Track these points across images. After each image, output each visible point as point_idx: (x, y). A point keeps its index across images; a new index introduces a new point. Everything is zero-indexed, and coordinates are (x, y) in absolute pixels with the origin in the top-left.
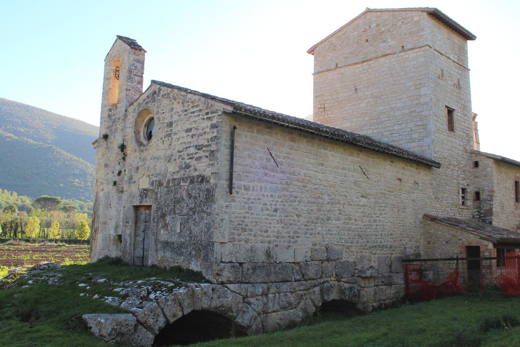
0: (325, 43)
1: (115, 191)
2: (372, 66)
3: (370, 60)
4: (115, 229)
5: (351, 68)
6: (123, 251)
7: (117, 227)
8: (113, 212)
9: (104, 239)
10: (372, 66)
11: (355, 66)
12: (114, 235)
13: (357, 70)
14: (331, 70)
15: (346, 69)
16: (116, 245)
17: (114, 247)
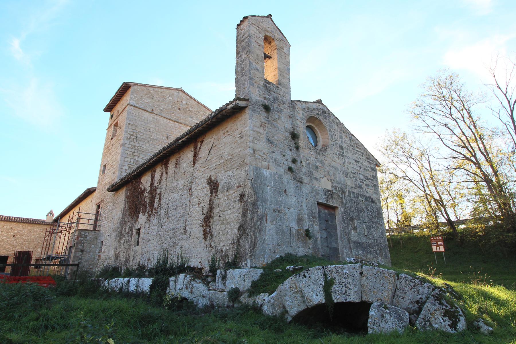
0: (143, 87)
1: (290, 177)
2: (182, 128)
3: (181, 123)
4: (298, 222)
5: (165, 120)
6: (314, 248)
7: (300, 220)
8: (292, 201)
9: (281, 232)
10: (182, 128)
11: (169, 121)
12: (297, 228)
13: (170, 125)
14: (147, 111)
15: (161, 118)
16: (303, 241)
17: (300, 243)
